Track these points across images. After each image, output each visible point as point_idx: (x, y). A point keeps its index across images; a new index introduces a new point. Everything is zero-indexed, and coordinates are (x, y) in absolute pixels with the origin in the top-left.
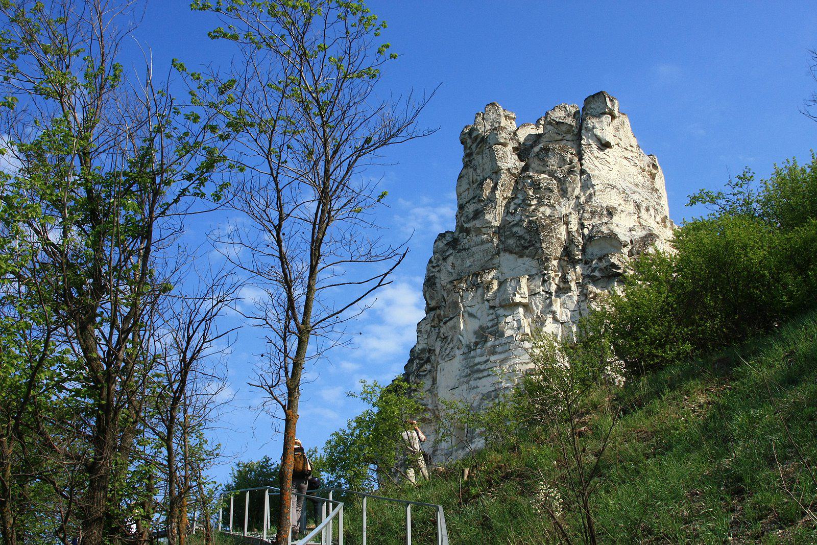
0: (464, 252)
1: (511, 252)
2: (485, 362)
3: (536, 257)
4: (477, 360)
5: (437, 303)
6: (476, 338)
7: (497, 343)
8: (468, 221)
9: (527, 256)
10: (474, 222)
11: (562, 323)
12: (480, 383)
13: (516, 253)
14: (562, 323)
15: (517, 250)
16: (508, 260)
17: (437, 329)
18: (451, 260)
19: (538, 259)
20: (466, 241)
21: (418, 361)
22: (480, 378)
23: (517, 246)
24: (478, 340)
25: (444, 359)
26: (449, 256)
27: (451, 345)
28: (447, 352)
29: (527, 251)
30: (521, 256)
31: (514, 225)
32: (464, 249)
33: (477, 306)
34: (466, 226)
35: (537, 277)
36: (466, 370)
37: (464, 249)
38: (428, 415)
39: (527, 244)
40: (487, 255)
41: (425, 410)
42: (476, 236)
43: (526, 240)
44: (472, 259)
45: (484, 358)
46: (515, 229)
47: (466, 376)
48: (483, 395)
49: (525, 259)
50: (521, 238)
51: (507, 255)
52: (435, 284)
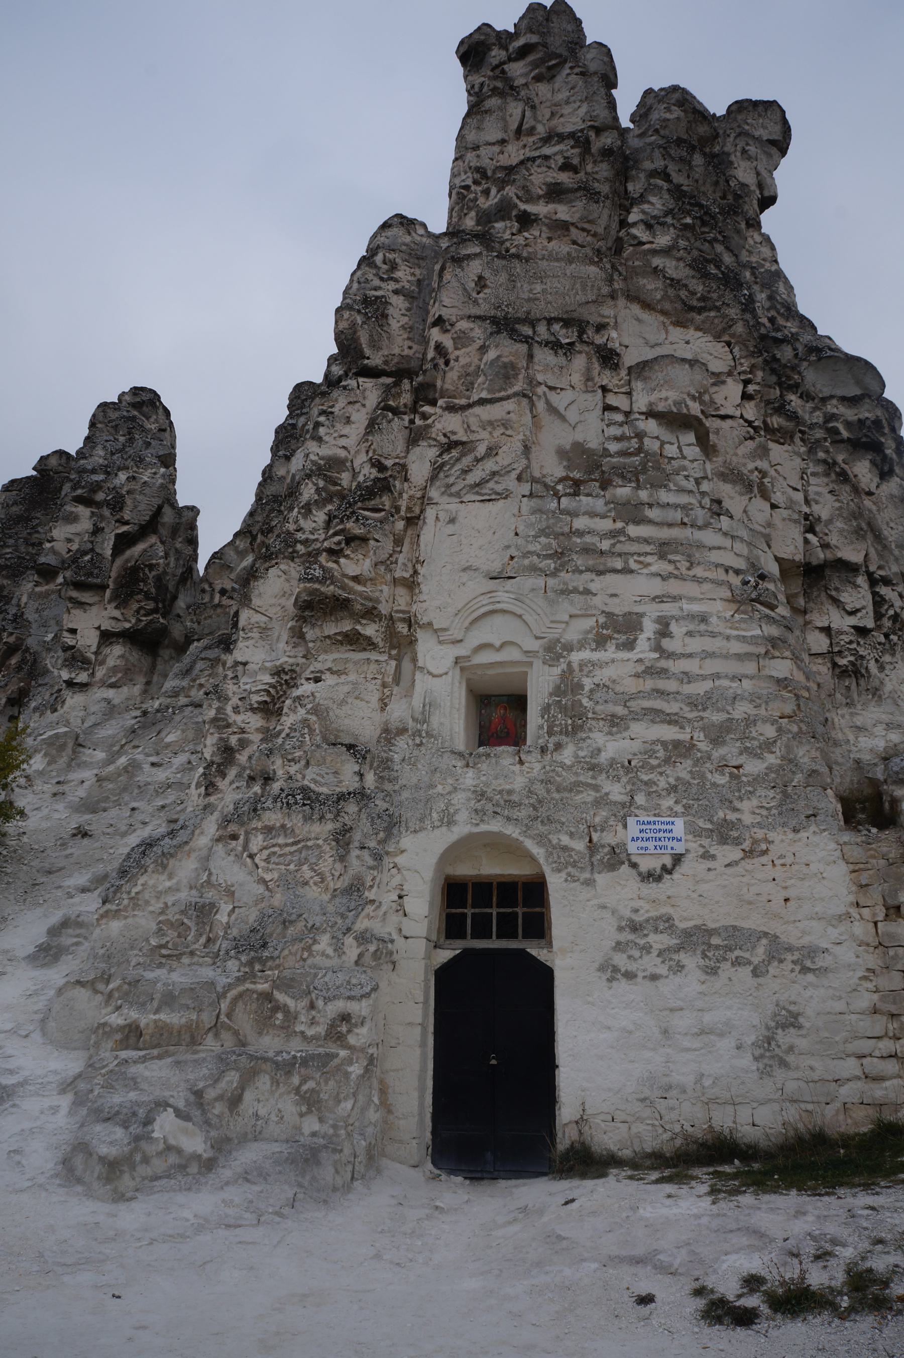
0: (516, 262)
1: (647, 306)
2: (613, 534)
3: (726, 338)
4: (580, 523)
5: (386, 362)
6: (567, 468)
7: (644, 495)
8: (530, 199)
9: (698, 329)
10: (551, 207)
11: (774, 506)
12: (598, 584)
13: (663, 313)
14: (774, 506)
15: (667, 306)
16: (638, 320)
17: (406, 418)
18: (475, 268)
19: (729, 344)
20: (519, 240)
21: (321, 483)
22: (600, 573)
23: (665, 297)
24: (576, 475)
25: (458, 494)
26: (469, 257)
27: (490, 465)
28: (472, 478)
29: (699, 318)
30: (678, 324)
31: (655, 252)
32: (517, 256)
33: (568, 395)
34: (523, 206)
35: (729, 380)
36: (543, 540)
37: (517, 256)
38: (370, 630)
39: (695, 303)
40: (584, 288)
41: (371, 614)
42: (550, 239)
43: (693, 293)
44: (538, 288)
45: (606, 525)
46: (657, 261)
47: (547, 557)
48: (609, 615)
49: (692, 334)
50: (674, 283)
51: (636, 309)
52: (385, 316)
